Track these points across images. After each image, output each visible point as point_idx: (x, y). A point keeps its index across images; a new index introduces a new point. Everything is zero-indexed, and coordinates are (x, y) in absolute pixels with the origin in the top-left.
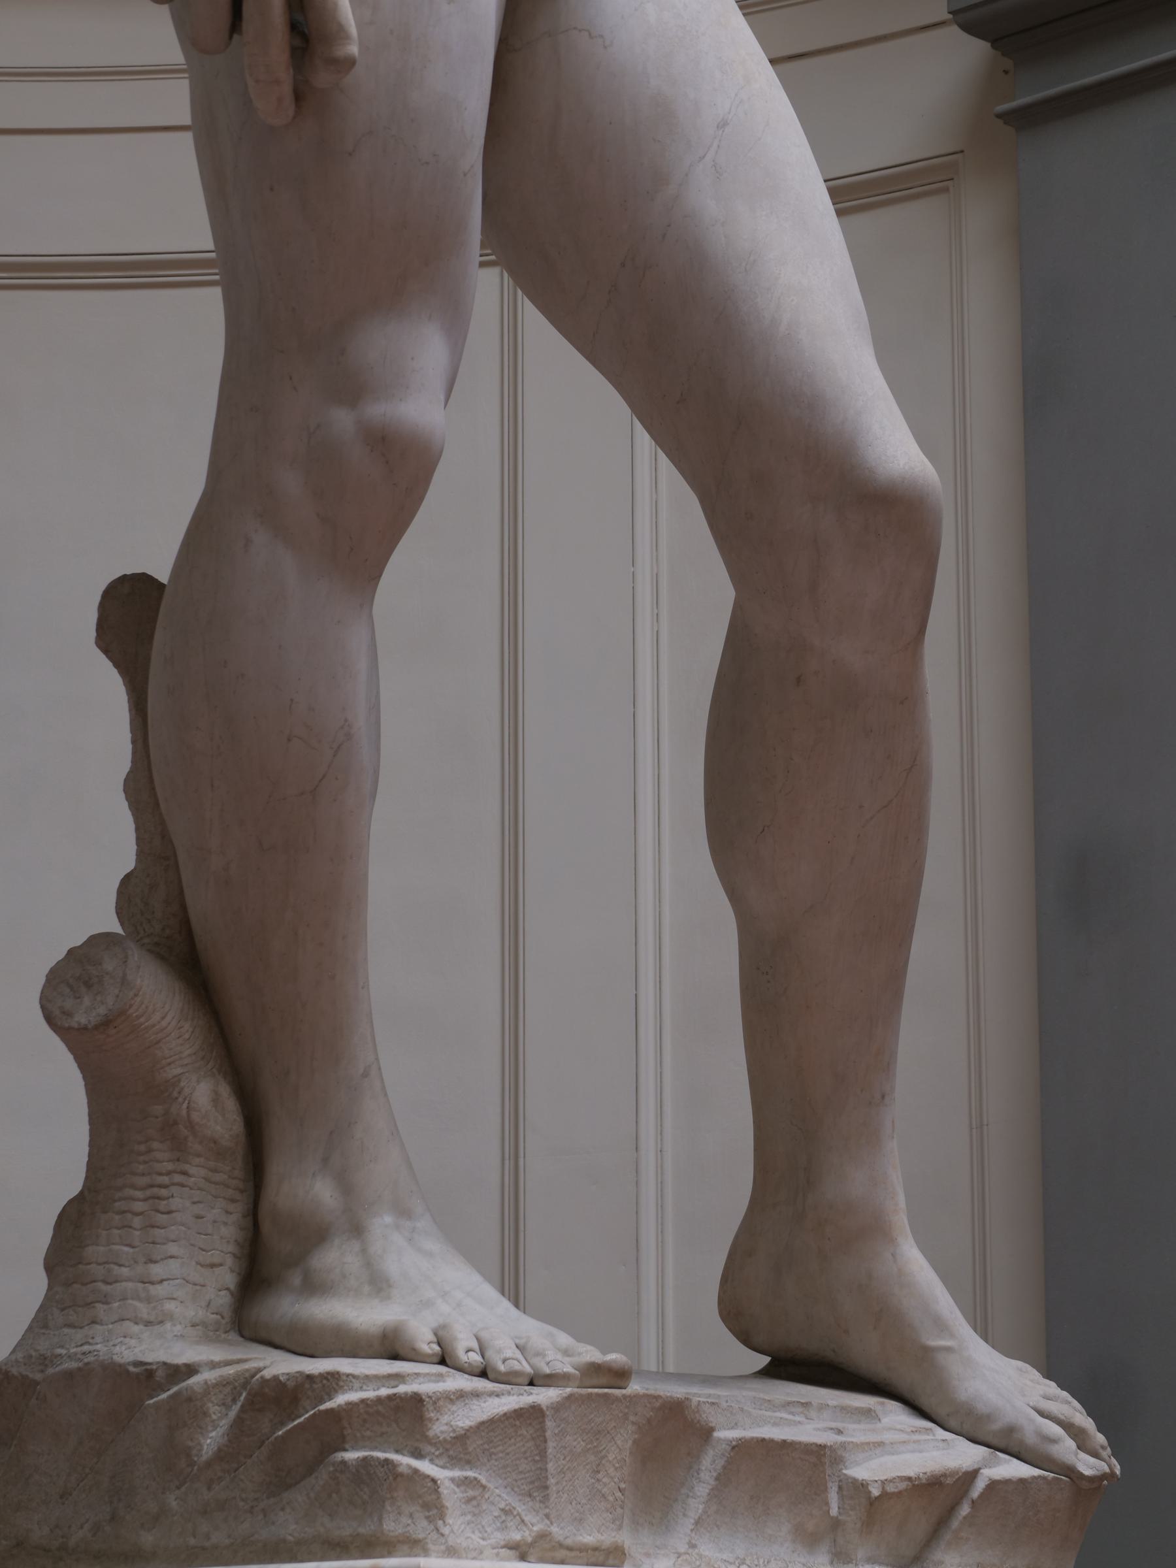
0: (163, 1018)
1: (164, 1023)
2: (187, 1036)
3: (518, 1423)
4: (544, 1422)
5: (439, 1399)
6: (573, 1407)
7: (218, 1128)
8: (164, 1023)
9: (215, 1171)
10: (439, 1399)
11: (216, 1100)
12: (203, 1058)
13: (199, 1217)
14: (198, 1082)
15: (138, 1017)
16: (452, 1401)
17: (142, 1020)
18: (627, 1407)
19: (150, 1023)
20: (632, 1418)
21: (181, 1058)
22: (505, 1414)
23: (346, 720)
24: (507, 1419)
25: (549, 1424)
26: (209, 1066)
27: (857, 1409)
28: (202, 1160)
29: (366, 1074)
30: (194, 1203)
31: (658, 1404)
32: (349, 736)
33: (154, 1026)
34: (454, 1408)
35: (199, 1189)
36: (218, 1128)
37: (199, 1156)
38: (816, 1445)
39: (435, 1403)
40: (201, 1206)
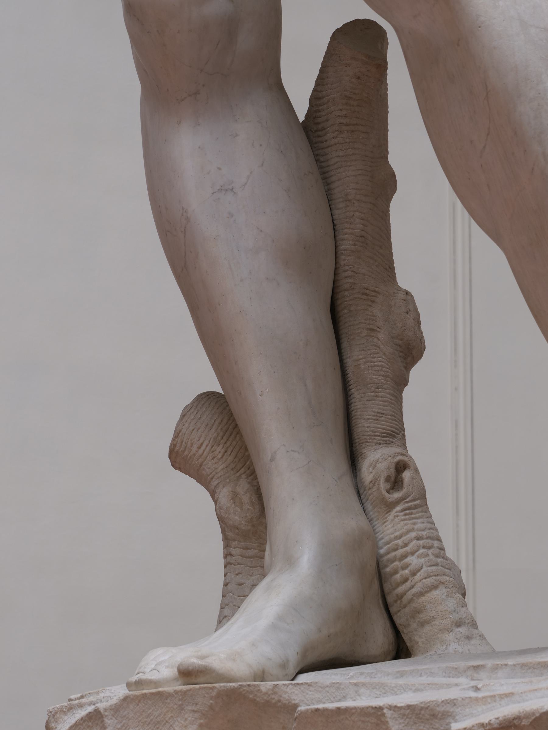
0: (199, 448)
1: (200, 451)
2: (219, 456)
3: (90, 724)
4: (103, 721)
5: (56, 713)
6: (131, 707)
7: (237, 518)
8: (200, 451)
9: (247, 549)
10: (56, 713)
11: (234, 496)
12: (232, 469)
13: (241, 584)
14: (224, 487)
15: (183, 452)
16: (65, 713)
17: (186, 453)
18: (179, 700)
19: (191, 453)
20: (190, 708)
21: (217, 473)
22: (82, 718)
23: (183, 209)
24: (84, 721)
25: (107, 721)
26: (238, 474)
27: (539, 663)
28: (236, 542)
29: (273, 459)
30: (237, 575)
31: (214, 694)
32: (188, 219)
33: (194, 455)
34: (65, 718)
35: (238, 564)
36: (237, 518)
37: (235, 540)
38: (372, 708)
39: (54, 716)
40: (240, 576)
